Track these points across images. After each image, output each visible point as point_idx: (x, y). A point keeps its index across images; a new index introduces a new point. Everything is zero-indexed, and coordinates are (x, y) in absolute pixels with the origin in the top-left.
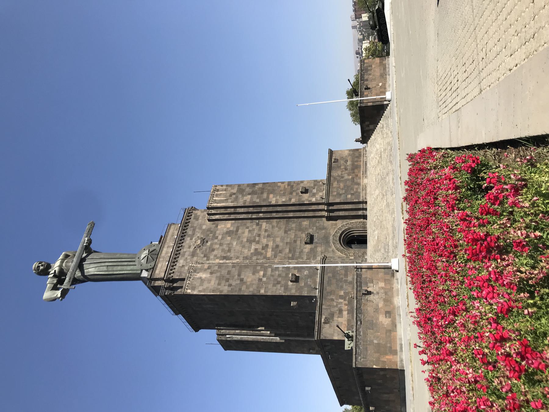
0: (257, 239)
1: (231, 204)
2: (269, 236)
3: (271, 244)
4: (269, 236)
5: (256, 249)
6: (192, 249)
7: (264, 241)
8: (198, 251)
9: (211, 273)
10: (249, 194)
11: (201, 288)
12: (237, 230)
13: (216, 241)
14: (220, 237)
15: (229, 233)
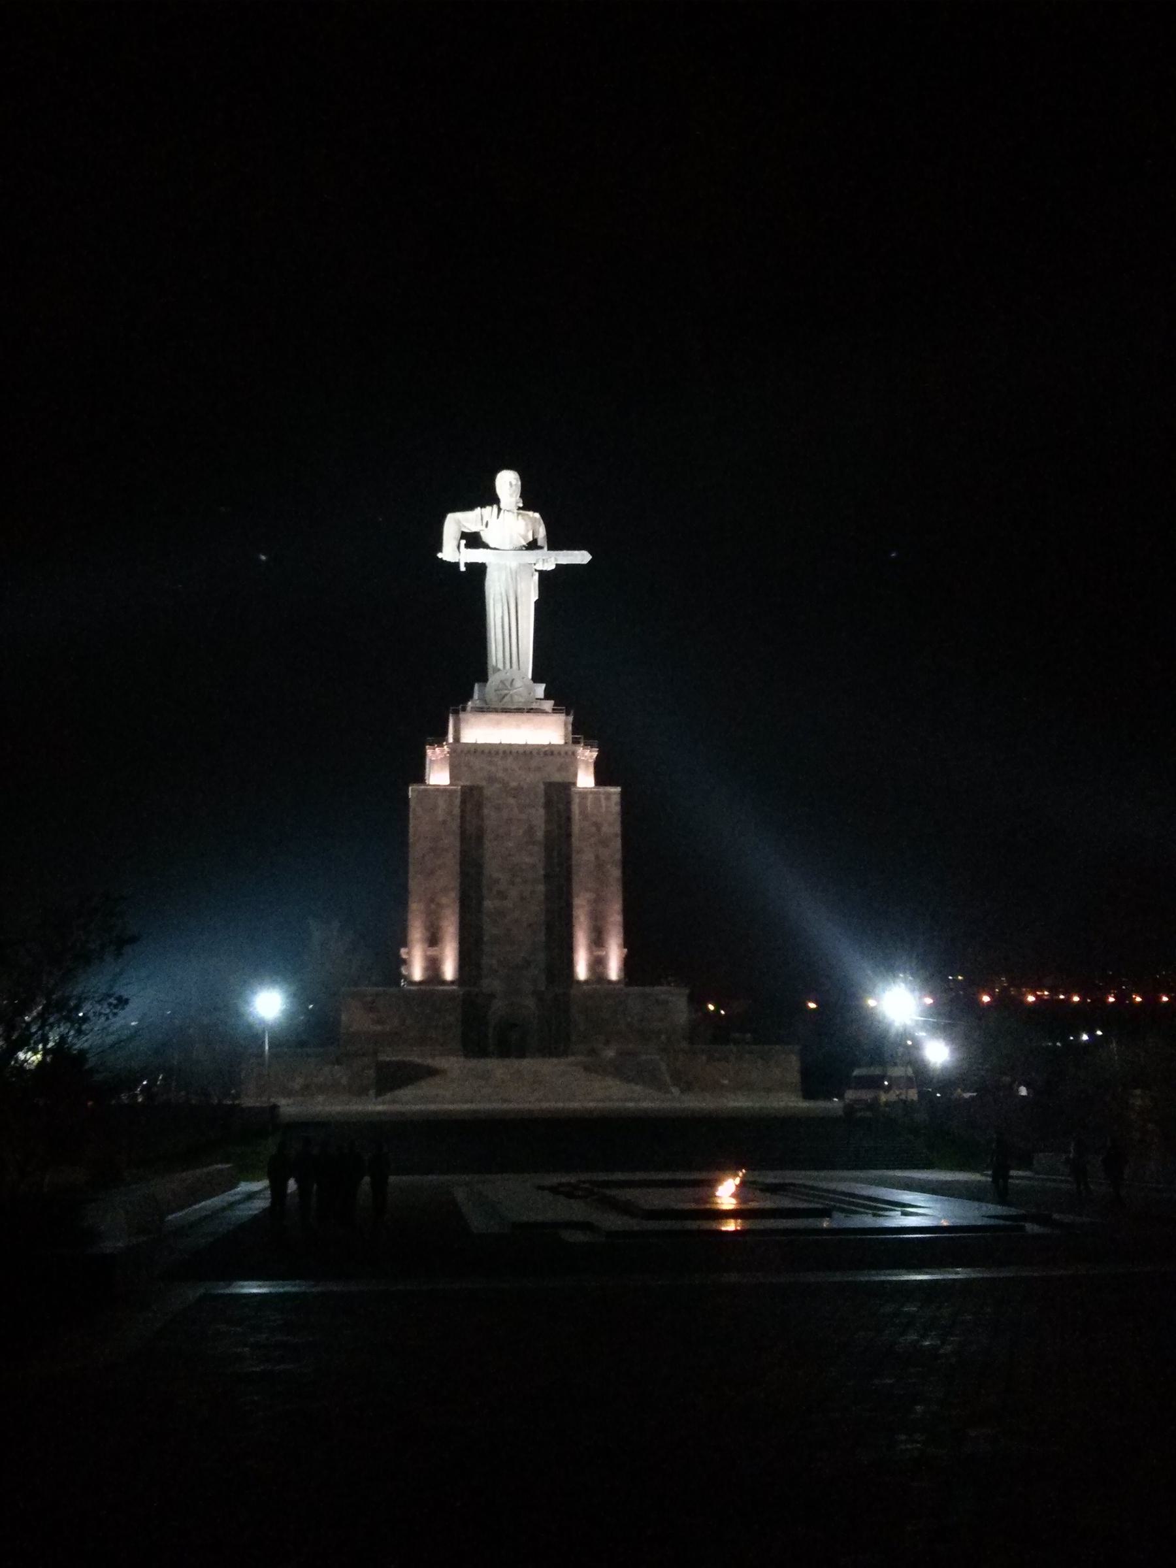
0: (518, 880)
1: (576, 829)
2: (523, 899)
3: (508, 904)
4: (523, 899)
5: (497, 881)
6: (500, 774)
7: (514, 893)
8: (497, 785)
9: (444, 822)
10: (597, 857)
11: (419, 809)
12: (534, 843)
13: (516, 810)
14: (524, 816)
15: (531, 830)
